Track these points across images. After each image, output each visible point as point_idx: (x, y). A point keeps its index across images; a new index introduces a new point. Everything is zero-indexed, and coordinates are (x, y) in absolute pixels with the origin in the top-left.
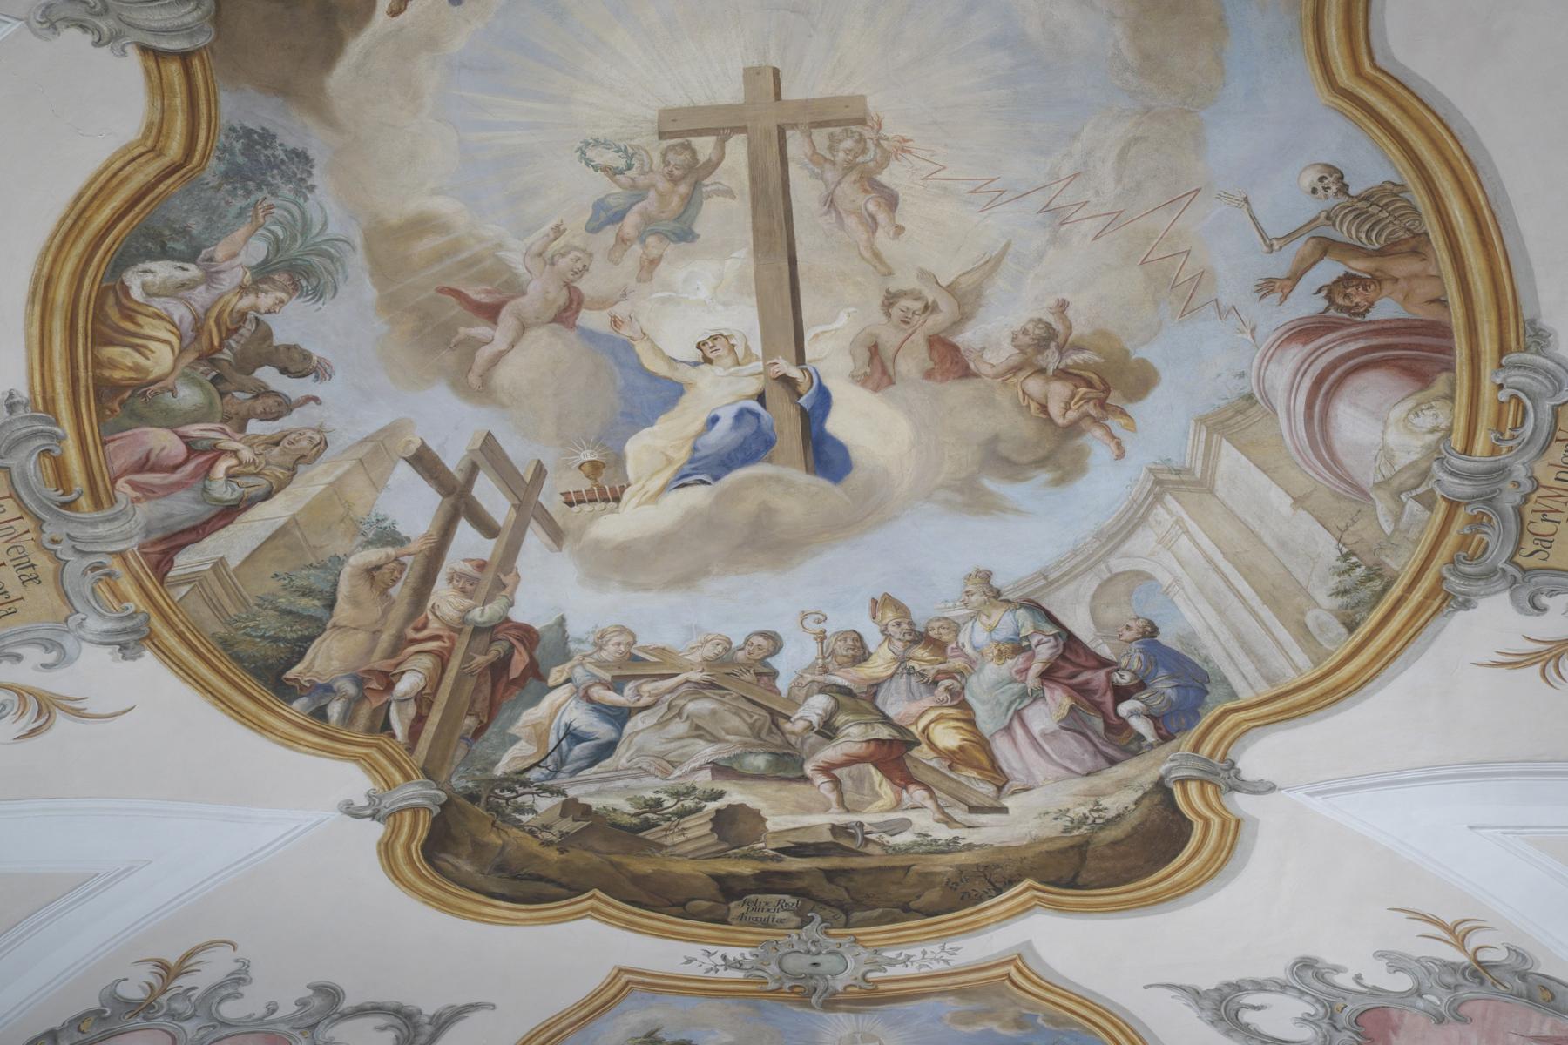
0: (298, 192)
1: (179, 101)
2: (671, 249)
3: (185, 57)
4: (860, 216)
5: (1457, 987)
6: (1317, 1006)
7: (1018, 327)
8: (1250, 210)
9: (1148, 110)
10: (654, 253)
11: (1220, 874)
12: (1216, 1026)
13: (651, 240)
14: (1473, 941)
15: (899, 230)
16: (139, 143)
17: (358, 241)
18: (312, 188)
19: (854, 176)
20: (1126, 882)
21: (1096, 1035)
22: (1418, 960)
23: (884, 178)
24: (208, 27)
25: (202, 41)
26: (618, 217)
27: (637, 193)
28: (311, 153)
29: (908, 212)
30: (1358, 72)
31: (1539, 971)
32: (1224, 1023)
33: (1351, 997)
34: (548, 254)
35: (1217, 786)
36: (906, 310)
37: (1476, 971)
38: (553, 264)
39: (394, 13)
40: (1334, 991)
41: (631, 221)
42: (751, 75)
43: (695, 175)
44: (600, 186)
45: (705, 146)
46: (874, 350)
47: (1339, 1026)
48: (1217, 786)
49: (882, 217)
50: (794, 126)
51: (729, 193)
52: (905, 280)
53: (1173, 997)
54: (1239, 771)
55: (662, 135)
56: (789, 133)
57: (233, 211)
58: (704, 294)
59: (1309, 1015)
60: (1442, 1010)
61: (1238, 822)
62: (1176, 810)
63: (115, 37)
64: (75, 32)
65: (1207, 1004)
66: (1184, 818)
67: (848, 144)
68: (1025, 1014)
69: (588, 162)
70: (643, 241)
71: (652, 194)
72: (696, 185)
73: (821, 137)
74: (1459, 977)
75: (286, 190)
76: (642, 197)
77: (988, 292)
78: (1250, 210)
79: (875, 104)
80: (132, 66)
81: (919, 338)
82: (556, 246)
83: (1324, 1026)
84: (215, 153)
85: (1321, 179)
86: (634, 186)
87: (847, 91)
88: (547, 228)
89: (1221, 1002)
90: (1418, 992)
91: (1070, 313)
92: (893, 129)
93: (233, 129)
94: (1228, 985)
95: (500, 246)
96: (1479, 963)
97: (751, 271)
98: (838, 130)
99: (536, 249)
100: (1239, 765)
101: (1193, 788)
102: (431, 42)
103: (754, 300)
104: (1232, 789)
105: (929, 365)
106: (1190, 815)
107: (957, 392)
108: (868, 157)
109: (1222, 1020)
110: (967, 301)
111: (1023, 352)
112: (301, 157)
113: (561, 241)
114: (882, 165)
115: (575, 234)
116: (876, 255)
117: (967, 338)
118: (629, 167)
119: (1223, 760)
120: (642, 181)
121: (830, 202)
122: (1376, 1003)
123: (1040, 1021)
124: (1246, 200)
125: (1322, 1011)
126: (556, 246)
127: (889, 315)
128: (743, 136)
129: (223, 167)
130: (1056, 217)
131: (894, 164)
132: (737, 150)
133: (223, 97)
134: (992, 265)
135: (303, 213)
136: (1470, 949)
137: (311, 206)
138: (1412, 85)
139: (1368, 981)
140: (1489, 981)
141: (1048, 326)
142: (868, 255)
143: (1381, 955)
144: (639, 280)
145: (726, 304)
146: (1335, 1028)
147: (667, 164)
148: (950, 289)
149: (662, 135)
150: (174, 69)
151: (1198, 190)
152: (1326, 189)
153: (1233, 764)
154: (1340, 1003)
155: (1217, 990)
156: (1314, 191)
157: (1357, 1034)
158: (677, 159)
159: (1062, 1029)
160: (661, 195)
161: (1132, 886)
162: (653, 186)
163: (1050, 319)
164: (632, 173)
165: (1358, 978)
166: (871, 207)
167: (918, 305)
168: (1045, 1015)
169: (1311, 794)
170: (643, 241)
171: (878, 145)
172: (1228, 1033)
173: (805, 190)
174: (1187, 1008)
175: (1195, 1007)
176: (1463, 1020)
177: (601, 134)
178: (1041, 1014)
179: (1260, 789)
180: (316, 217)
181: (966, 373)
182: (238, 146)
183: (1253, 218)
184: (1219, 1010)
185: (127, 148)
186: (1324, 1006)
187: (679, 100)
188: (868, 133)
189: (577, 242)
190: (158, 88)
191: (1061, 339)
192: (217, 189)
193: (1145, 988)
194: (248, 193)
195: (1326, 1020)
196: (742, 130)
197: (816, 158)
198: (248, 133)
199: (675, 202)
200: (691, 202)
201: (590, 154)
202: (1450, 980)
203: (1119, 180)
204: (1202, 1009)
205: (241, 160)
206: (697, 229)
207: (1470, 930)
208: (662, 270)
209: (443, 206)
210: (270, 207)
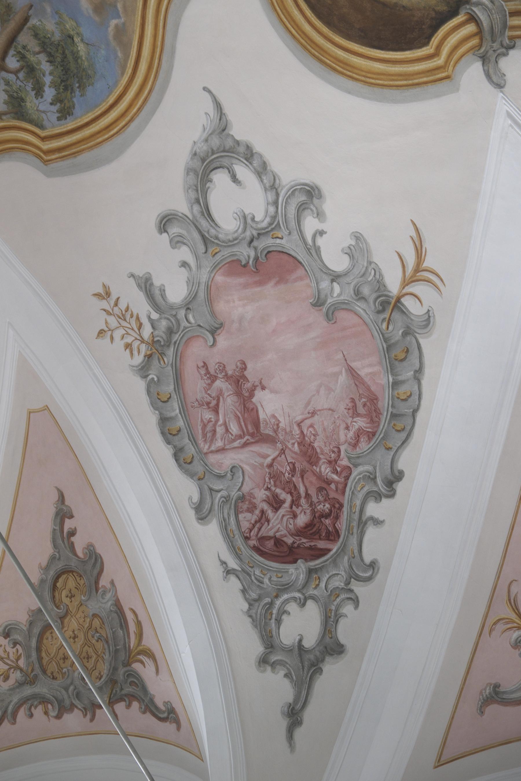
5: (363, 299)
6: (268, 219)
11: (377, 90)
12: (192, 159)
14: (417, 288)
20: (328, 23)
21: (123, 74)
22: (370, 263)
31: (421, 341)
32: (200, 163)
33: (295, 236)
35: (480, 45)
37: (389, 303)
40: (293, 224)
47: (255, 243)
48: (480, 45)
53: (206, 114)
54: (505, 55)
59: (253, 219)
60: (329, 301)
61: (448, 77)
62: (435, 28)
65: (215, 142)
66: (428, 39)
68: (116, 7)
74: (374, 296)
83: (248, 234)
89: (224, 151)
90: (335, 277)
94: (248, 148)
96: (398, 300)
100: (512, 52)
101: (471, 28)
104: (484, 59)
106: (435, 40)
109: (203, 160)
119: (511, 38)
122: (302, 255)
123: (114, 22)
125: (264, 224)
136: (408, 289)
139: (320, 241)
140: (386, 315)
143: (358, 237)
146: (251, 241)
153: (513, 47)
154: (283, 232)
155: (238, 143)
157: (256, 259)
159: (113, 43)
161: (325, 29)
165: (322, 233)
168: (124, 24)
169: (509, 115)
172: (189, 170)
174: (200, 129)
175: (205, 135)
176: (330, 317)
178: (123, 20)
179: (495, 78)
184: (213, 153)
186: (270, 224)
193: (205, 89)
195: (255, 233)
202: (366, 291)
204: (206, 140)
207: (428, 281)
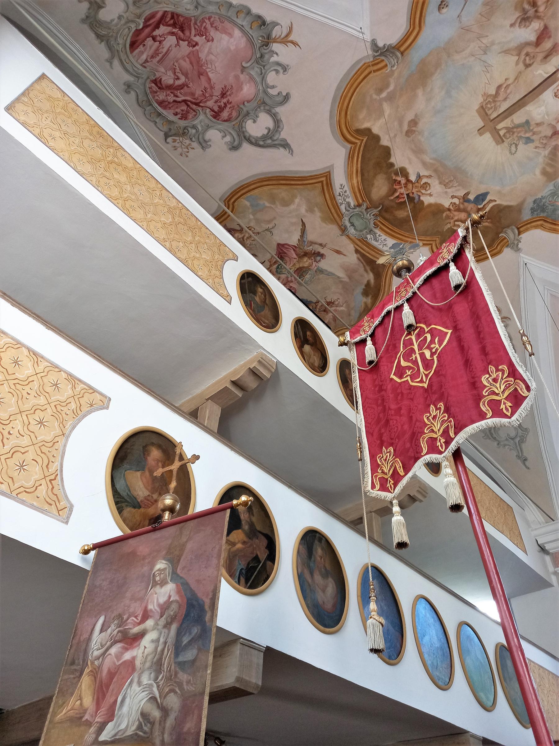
0: (544, 198)
1: (529, 226)
2: (532, 123)
3: (518, 229)
4: (506, 91)
7: (524, 29)
8: (461, 13)
9: (449, 56)
10: (535, 125)
13: (531, 128)
15: (506, 80)
16: (540, 228)
17: (553, 182)
18: (542, 196)
19: (496, 99)
23: (494, 93)
24: (511, 227)
25: (514, 227)
26: (528, 138)
27: (520, 138)
28: (533, 200)
29: (500, 82)
30: (414, 28)
34: (544, 146)
36: (530, 60)
38: (546, 144)
39: (496, 201)
41: (527, 135)
42: (481, 134)
43: (510, 130)
44: (521, 146)
45: (502, 133)
46: (546, 57)
49: (504, 86)
50: (489, 119)
51: (512, 121)
52: (521, 66)
55: (503, 141)
56: (492, 119)
57: (552, 207)
58: (543, 108)
63: (518, 240)
64: (519, 246)
67: (489, 106)
69: (516, 152)
70: (533, 129)
71: (519, 135)
72: (513, 128)
73: (489, 112)
75: (544, 201)
76: (521, 137)
77: (516, 45)
78: (461, 13)
79: (477, 107)
80: (523, 236)
81: (538, 50)
82: (540, 146)
84: (539, 216)
85: (443, 8)
86: (519, 139)
87: (477, 115)
88: (537, 150)
91: (513, 22)
92: (481, 99)
93: (532, 215)
95: (545, 156)
97: (532, 103)
98: (486, 110)
99: (543, 149)
102: (499, 192)
103: (541, 97)
105: (546, 40)
107: (552, 25)
108: (489, 99)
110: (519, 49)
111: (532, 20)
112: (534, 202)
113: (539, 145)
114: (491, 95)
115: (537, 143)
116: (516, 79)
117: (533, 38)
118: (514, 143)
120: (516, 139)
121: (505, 99)
124: (458, 17)
126: (540, 146)
127: (533, 63)
128: (497, 127)
129: (542, 213)
130: (486, 50)
131: (489, 93)
132: (499, 126)
133: (525, 219)
134: (507, 52)
135: (549, 195)
137: (546, 195)
138: (409, 17)
141: (520, 22)
142: (517, 81)
144: (544, 124)
145: (544, 101)
147: (510, 137)
148: (519, 55)
149: (503, 141)
150: (521, 229)
151: (462, 29)
152: (445, 5)
156: (447, 6)
158: (508, 135)
160: (518, 133)
162: (517, 136)
163: (517, 25)
164: (515, 142)
166: (503, 90)
167: (527, 58)
170: (533, 129)
171: (486, 100)
173: (505, 106)
177: (508, 153)
180: (549, 193)
181: (546, 27)
182: (536, 213)
183: (462, 10)
185: (542, 230)
187: (494, 143)
188: (484, 103)
189: (538, 142)
190: (527, 230)
191: (522, 16)
192: (548, 212)
194: (547, 207)
196: (495, 128)
197: (495, 109)
198: (532, 212)
199: (519, 129)
200: (518, 126)
201: (514, 152)
203: (469, 46)
205: (539, 211)
206: (524, 121)
208: (538, 121)
209: (538, 172)
210: (550, 201)
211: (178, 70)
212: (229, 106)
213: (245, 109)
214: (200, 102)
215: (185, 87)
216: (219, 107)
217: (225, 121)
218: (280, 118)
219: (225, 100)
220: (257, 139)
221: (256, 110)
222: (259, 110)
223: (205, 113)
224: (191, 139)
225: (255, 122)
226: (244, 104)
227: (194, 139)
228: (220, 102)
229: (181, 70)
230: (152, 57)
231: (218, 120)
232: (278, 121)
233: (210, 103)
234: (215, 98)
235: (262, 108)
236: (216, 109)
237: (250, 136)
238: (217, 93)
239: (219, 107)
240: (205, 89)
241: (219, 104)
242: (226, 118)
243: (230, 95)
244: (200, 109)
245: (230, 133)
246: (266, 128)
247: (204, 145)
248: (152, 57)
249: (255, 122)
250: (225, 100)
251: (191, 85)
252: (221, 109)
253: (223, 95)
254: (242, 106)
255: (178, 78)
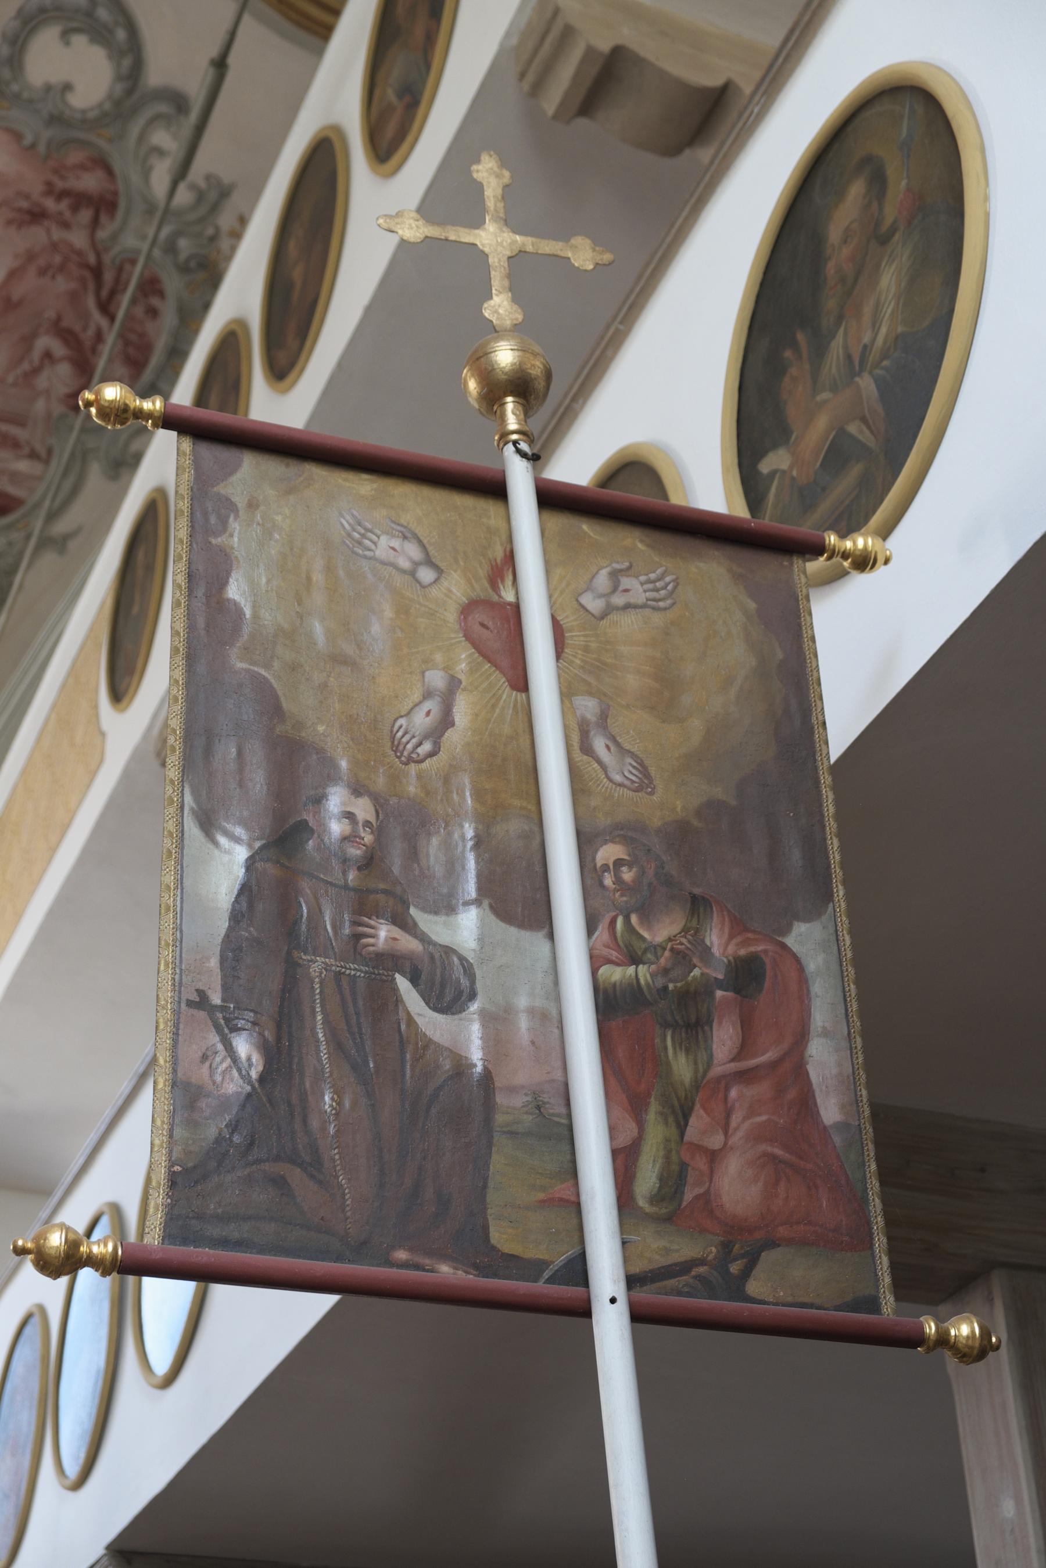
211: (26, 366)
212: (60, 184)
213: (47, 134)
214: (88, 266)
215: (65, 323)
216: (75, 208)
217: (109, 172)
218: (16, 18)
219: (50, 204)
220: (116, 53)
221: (31, 101)
222: (25, 95)
223: (114, 237)
224: (213, 239)
225: (67, 87)
226: (33, 146)
227: (210, 231)
228: (61, 213)
229: (21, 360)
230: (16, 445)
231: (115, 193)
232: (25, 23)
233: (78, 239)
234: (57, 234)
235: (15, 88)
236: (85, 215)
237: (119, 78)
238: (37, 236)
239: (75, 208)
240: (43, 272)
241: (68, 214)
242: (100, 173)
243: (27, 197)
244: (107, 259)
245: (142, 138)
246: (67, 43)
247: (213, 196)
248: (16, 445)
249: (67, 87)
250: (50, 204)
251: (50, 314)
252: (79, 200)
253: (36, 216)
254: (42, 148)
255: (48, 355)
